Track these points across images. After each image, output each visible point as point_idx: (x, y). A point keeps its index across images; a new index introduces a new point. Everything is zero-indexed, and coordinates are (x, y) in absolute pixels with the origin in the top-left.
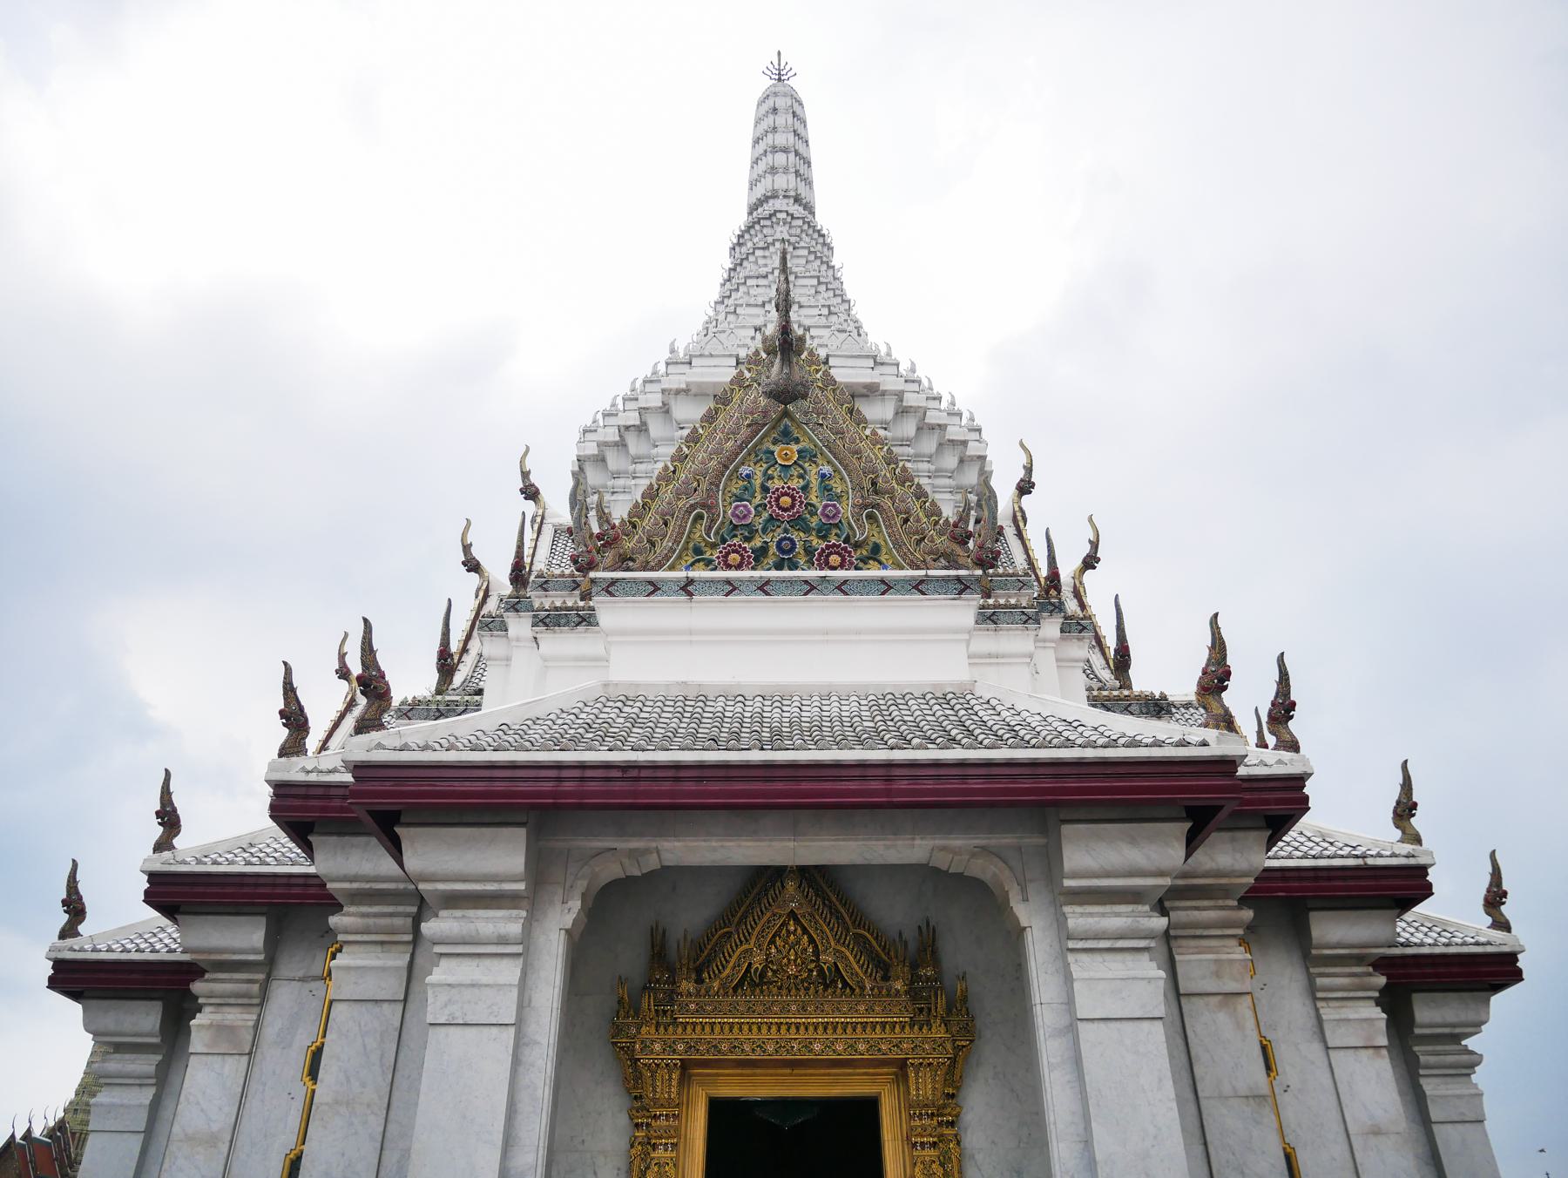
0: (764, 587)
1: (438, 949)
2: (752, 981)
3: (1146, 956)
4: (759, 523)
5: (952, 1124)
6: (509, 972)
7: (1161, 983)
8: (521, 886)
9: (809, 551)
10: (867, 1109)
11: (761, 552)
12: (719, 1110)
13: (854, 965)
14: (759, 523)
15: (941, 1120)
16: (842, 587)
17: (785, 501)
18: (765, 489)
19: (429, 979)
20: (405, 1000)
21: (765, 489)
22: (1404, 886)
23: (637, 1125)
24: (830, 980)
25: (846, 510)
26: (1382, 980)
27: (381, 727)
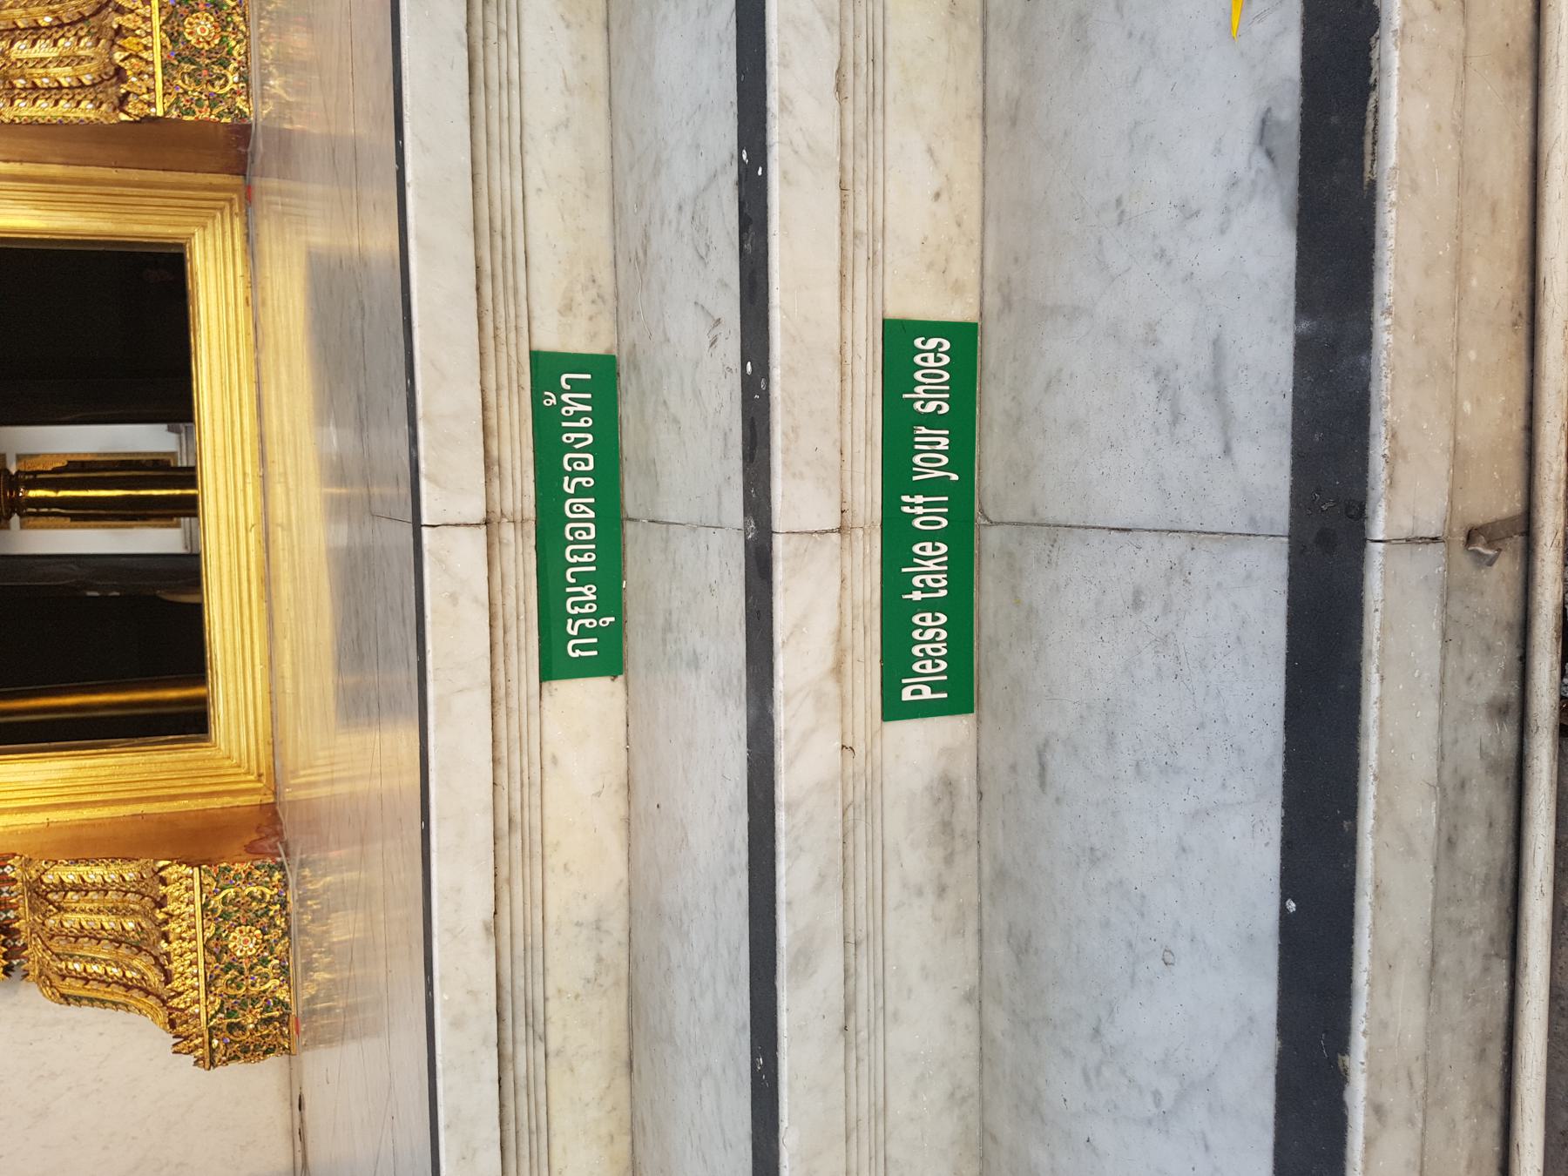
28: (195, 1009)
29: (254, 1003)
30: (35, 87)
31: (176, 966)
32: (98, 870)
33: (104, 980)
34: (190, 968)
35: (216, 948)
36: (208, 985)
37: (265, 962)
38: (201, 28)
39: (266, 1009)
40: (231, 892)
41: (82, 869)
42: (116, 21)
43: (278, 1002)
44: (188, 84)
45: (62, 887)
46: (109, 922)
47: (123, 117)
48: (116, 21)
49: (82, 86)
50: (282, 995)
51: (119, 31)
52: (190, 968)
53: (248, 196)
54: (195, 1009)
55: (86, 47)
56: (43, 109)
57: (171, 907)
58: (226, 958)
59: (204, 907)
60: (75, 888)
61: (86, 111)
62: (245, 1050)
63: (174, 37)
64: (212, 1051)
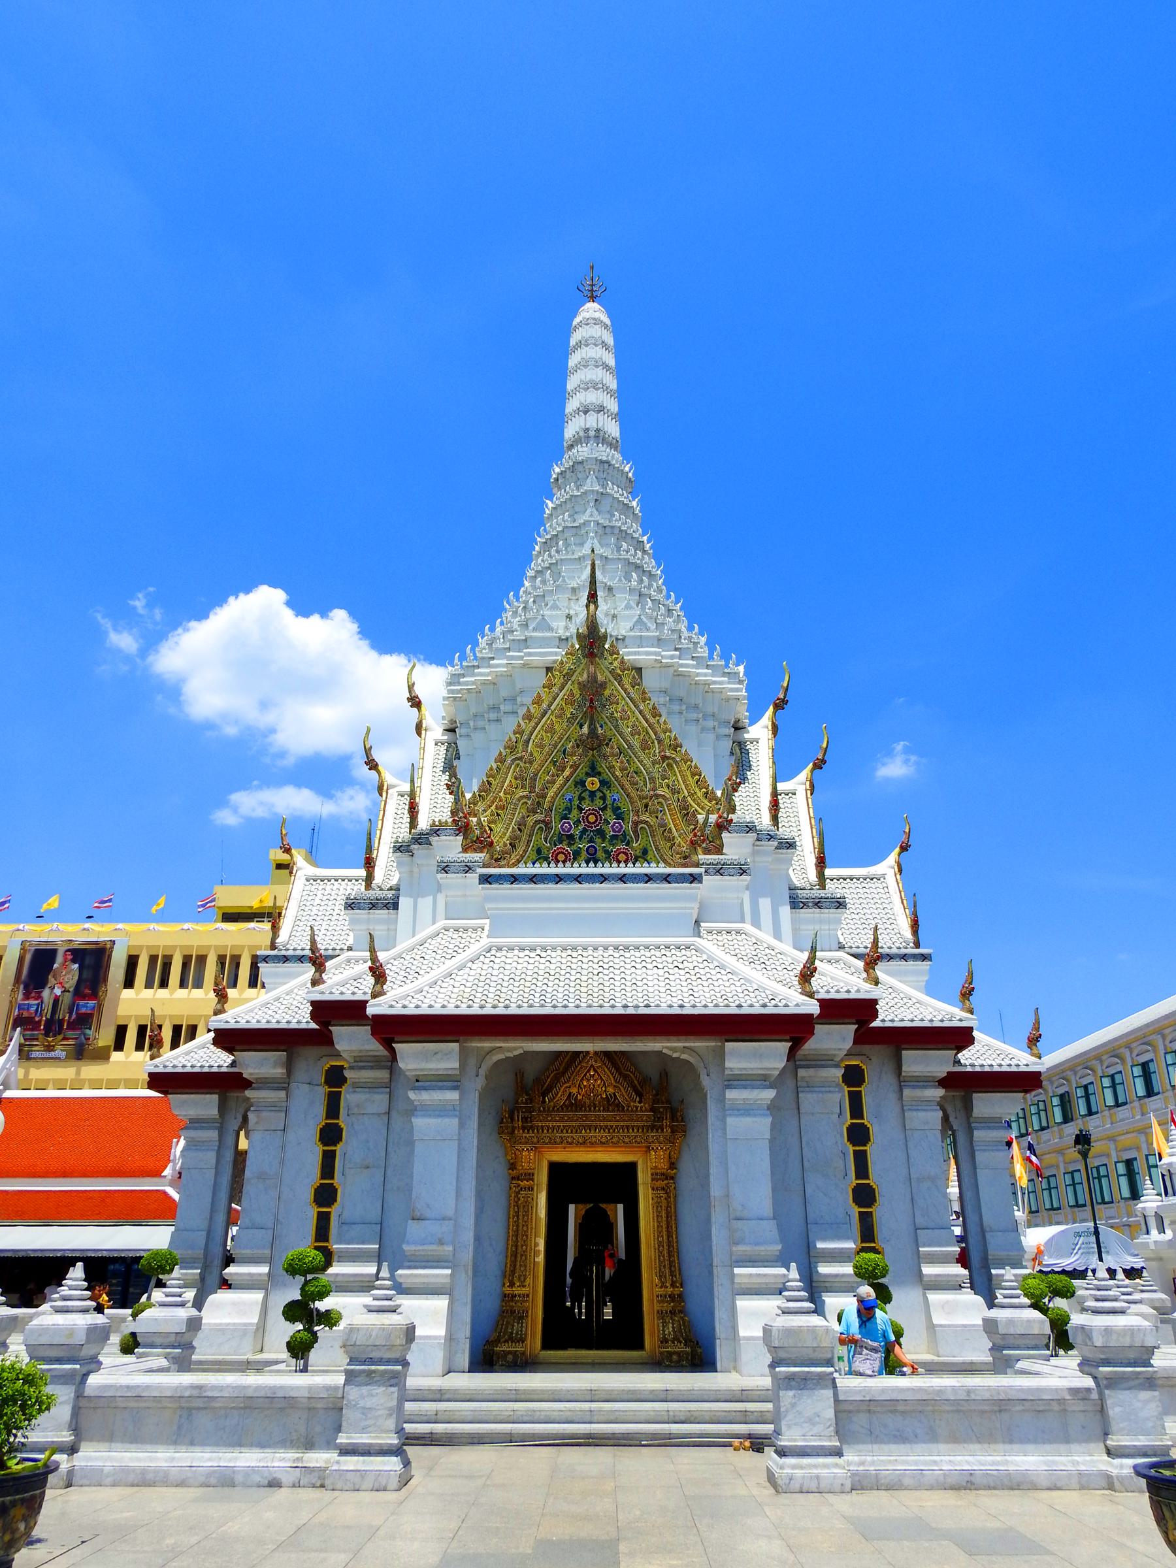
0: (578, 879)
2: (573, 1105)
4: (577, 833)
9: (607, 852)
10: (631, 1168)
11: (577, 854)
13: (623, 1095)
14: (577, 833)
16: (623, 878)
17: (592, 819)
18: (580, 809)
21: (580, 809)
22: (961, 1038)
24: (611, 1104)
25: (629, 828)
26: (941, 1092)
27: (382, 993)
34: (505, 1347)
38: (675, 1357)
52: (505, 1347)
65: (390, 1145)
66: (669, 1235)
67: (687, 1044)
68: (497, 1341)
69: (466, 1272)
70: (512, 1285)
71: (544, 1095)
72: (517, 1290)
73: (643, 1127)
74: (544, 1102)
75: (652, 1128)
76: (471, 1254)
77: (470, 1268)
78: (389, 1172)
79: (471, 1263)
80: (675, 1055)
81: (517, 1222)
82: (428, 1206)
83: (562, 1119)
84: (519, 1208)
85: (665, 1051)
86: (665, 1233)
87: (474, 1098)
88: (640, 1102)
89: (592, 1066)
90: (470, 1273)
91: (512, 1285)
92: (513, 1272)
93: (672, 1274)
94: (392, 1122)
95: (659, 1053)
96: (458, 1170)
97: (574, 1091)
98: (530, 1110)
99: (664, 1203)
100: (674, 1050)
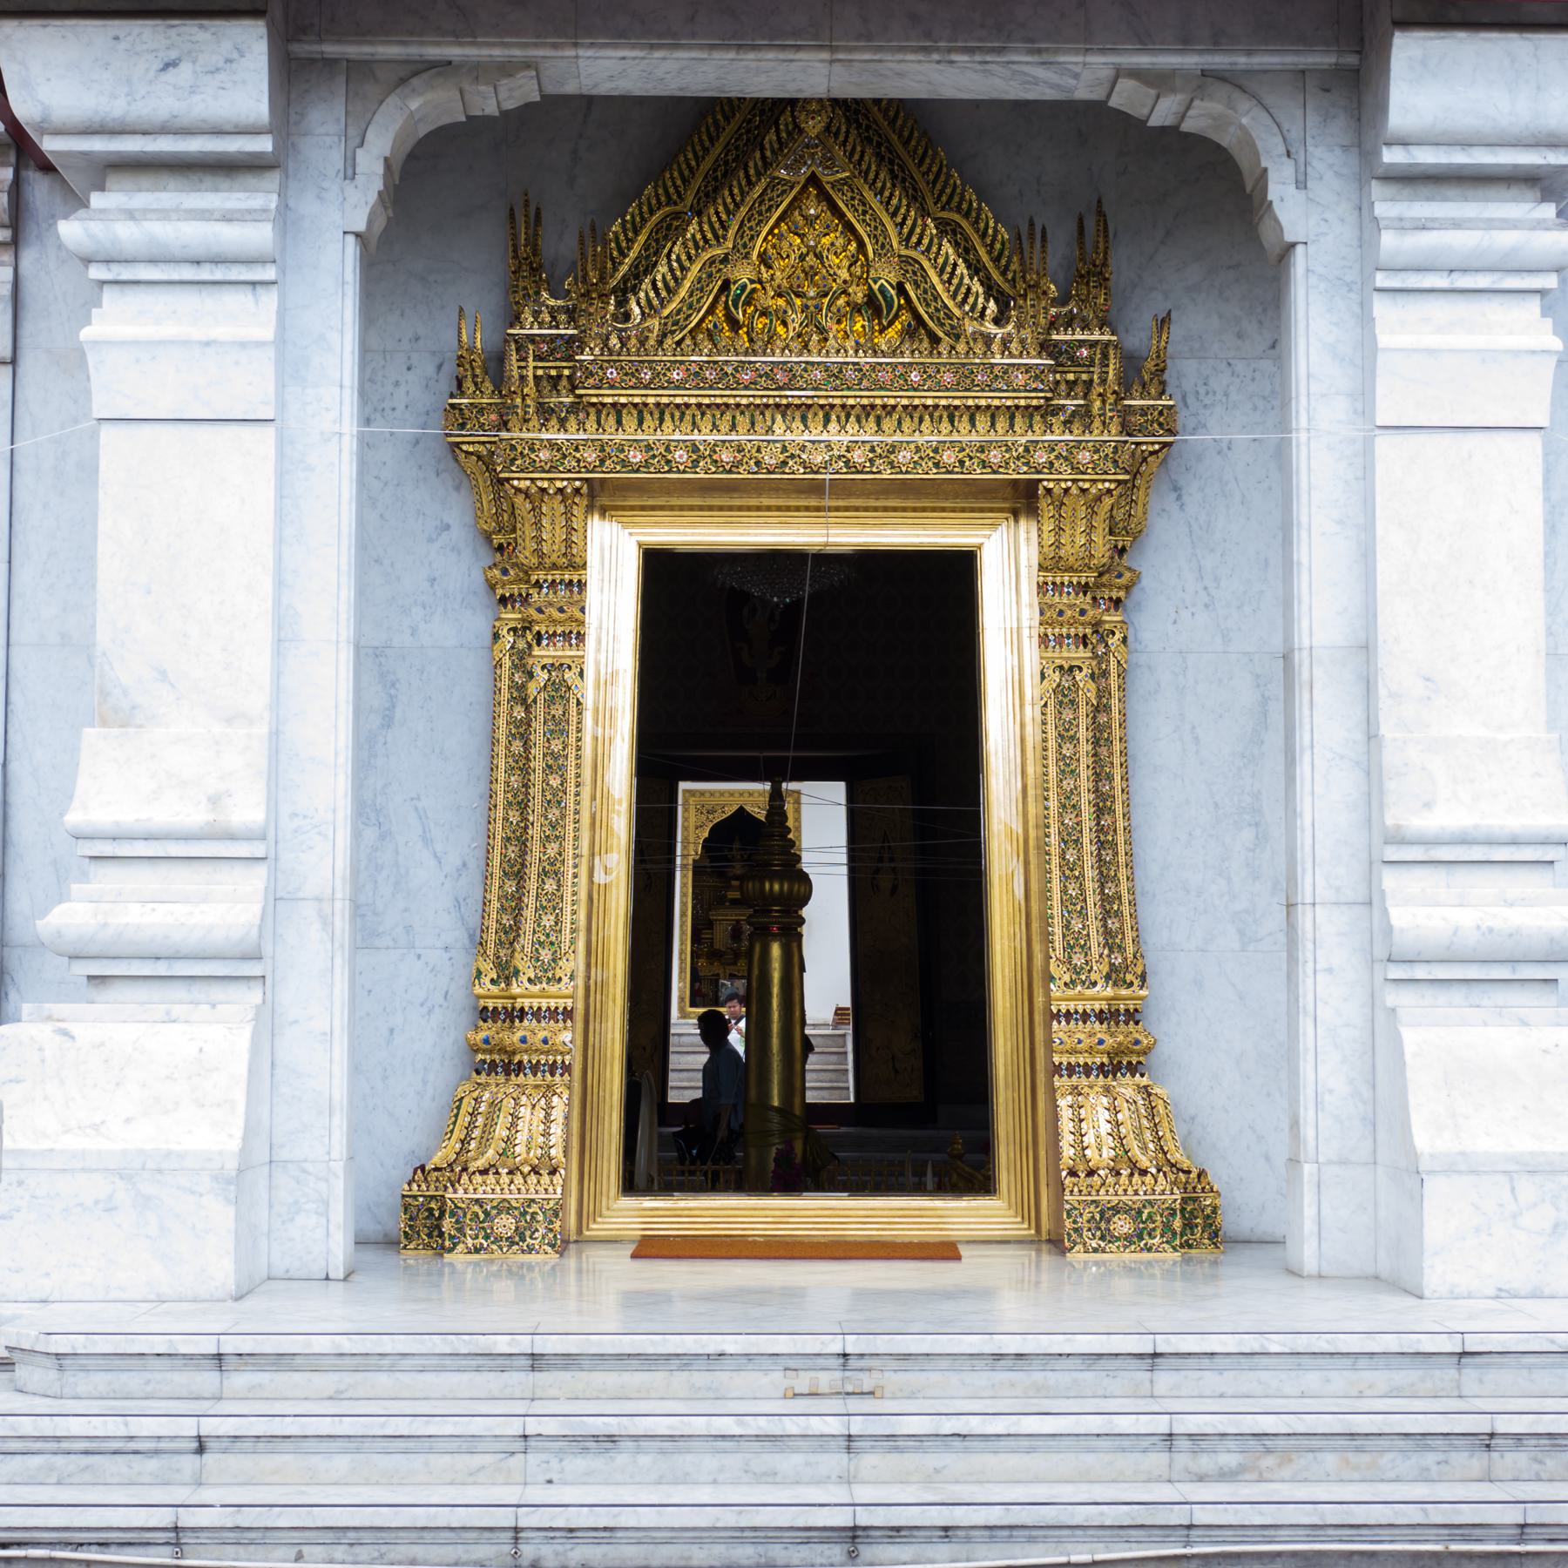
1: (96, 272)
3: (1534, 304)
5: (1117, 603)
6: (248, 317)
7: (1548, 367)
8: (264, 144)
10: (955, 574)
12: (664, 573)
15: (1094, 598)
19: (86, 333)
20: (14, 362)
23: (503, 600)
28: (461, 1191)
29: (458, 1230)
30: (1081, 1121)
31: (491, 1178)
32: (559, 1132)
33: (470, 1127)
35: (504, 1207)
36: (477, 1201)
37: (487, 1237)
38: (1122, 1225)
39: (451, 1237)
40: (540, 1217)
41: (561, 1120)
42: (1125, 1173)
43: (455, 1245)
44: (1086, 1216)
45: (549, 1108)
46: (521, 1138)
47: (1064, 1174)
48: (1125, 1173)
49: (1084, 1149)
50: (460, 1247)
51: (1118, 1174)
53: (1032, 1242)
54: (461, 1191)
55: (1107, 1153)
56: (1066, 1126)
57: (533, 1178)
58: (494, 1212)
59: (533, 1200)
60: (548, 1115)
61: (1068, 1152)
62: (411, 1219)
63: (1116, 1210)
64: (415, 1197)
65: (25, 481)
66: (1102, 808)
67: (1218, 61)
68: (458, 1169)
69: (327, 922)
70: (507, 973)
71: (625, 291)
72: (524, 992)
73: (1012, 412)
74: (627, 317)
75: (1048, 411)
76: (342, 862)
77: (342, 908)
78: (24, 577)
79: (342, 892)
80: (1163, 113)
81: (522, 765)
82: (163, 675)
83: (696, 377)
84: (530, 710)
85: (1127, 97)
86: (1085, 799)
87: (333, 271)
88: (997, 321)
89: (813, 180)
90: (342, 924)
91: (507, 973)
92: (510, 934)
93: (1111, 941)
94: (27, 393)
95: (1088, 121)
96: (279, 541)
97: (742, 274)
98: (572, 345)
99: (1088, 690)
100: (1160, 81)
